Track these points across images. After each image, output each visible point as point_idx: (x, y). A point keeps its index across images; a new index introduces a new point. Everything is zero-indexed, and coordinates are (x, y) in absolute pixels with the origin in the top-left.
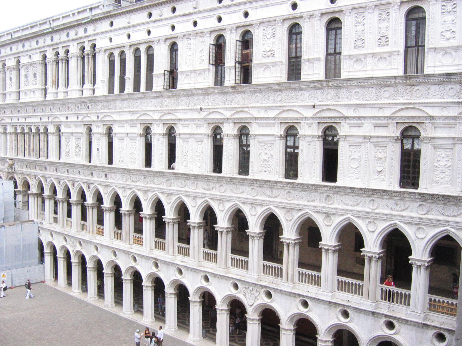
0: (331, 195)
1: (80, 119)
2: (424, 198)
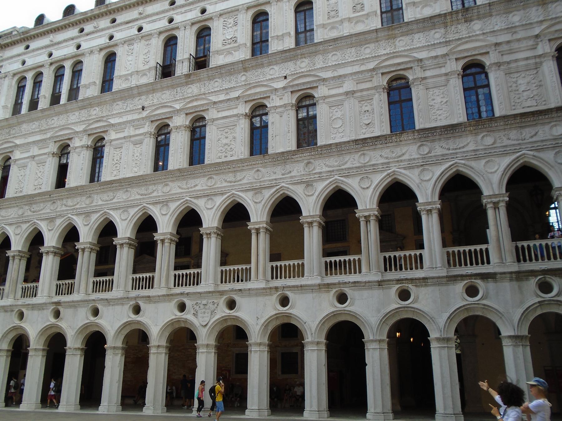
0: (311, 161)
2: (425, 135)
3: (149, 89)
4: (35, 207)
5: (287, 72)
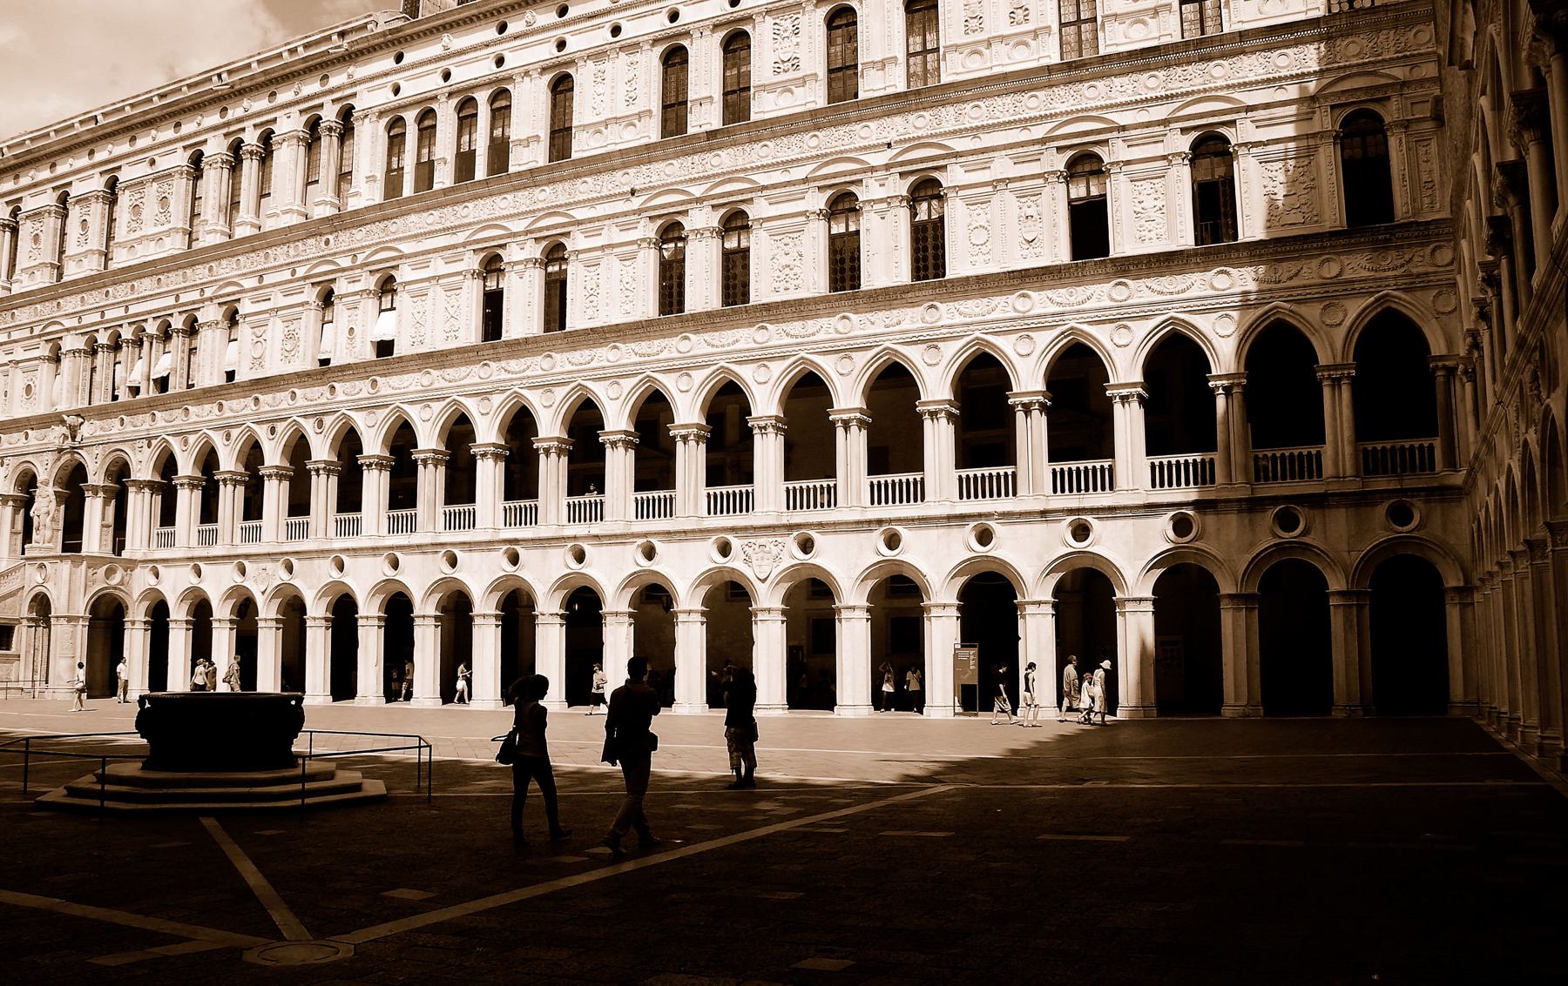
1: (301, 272)
3: (643, 155)
4: (451, 373)
5: (892, 136)
